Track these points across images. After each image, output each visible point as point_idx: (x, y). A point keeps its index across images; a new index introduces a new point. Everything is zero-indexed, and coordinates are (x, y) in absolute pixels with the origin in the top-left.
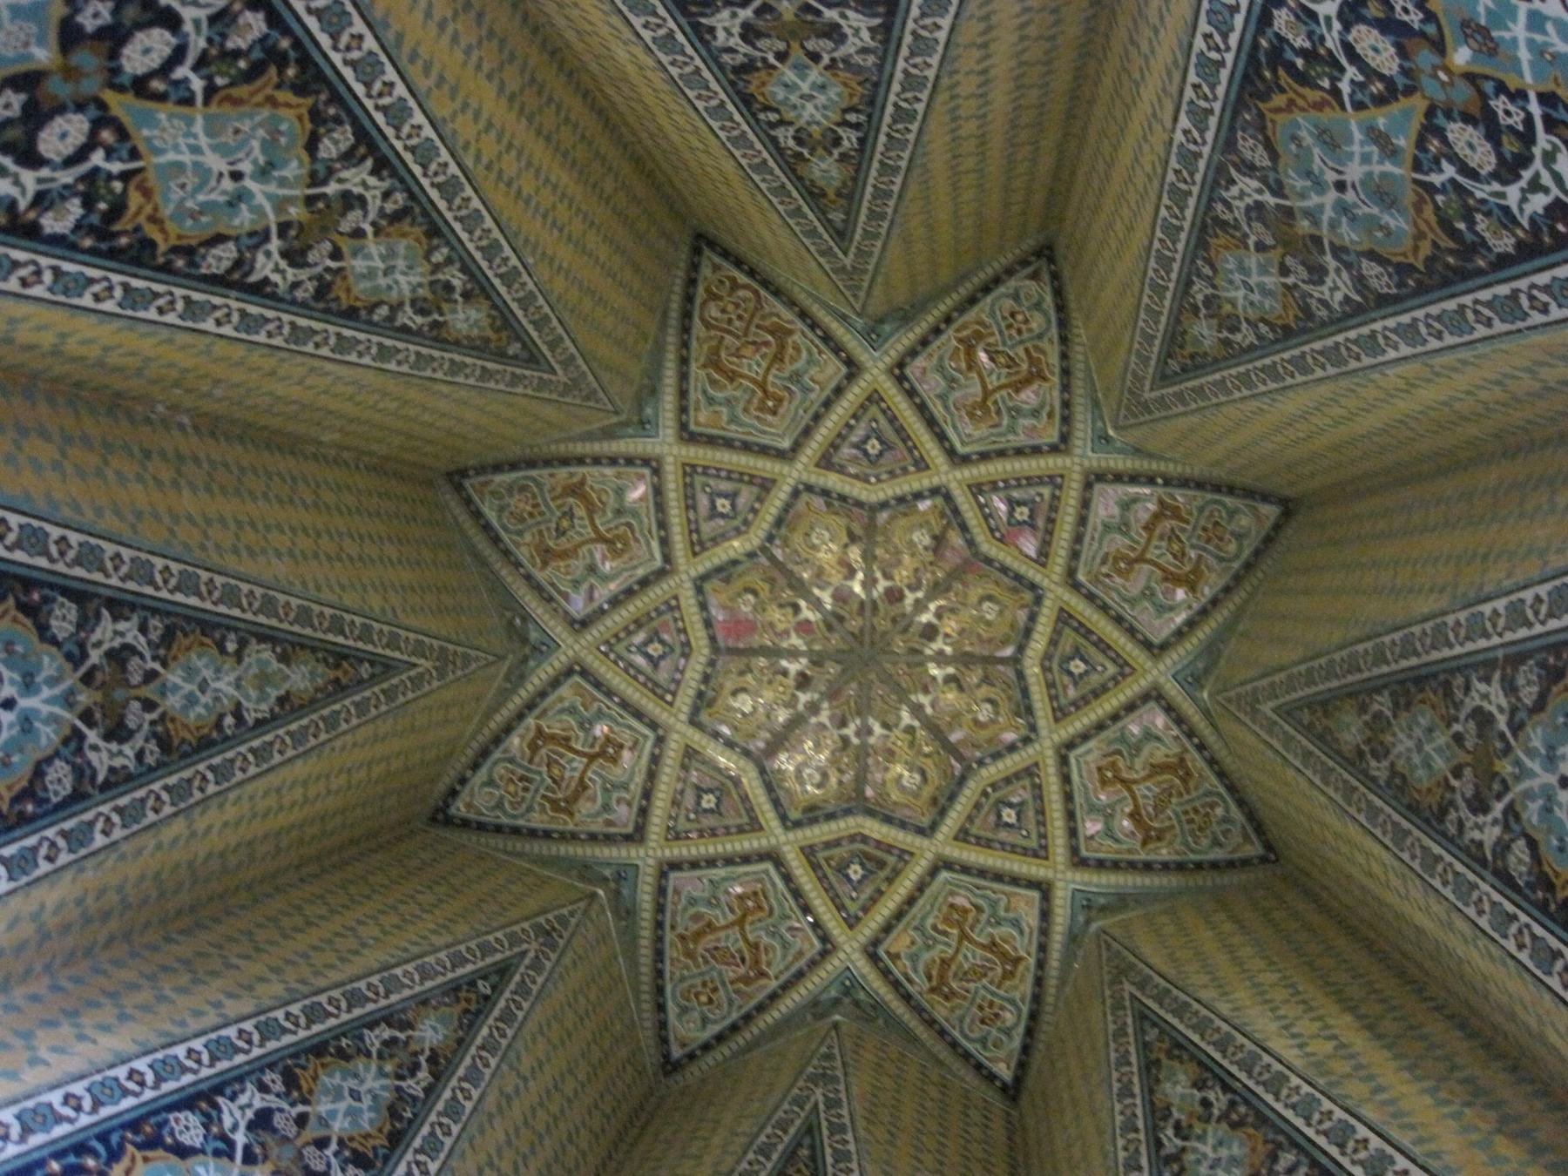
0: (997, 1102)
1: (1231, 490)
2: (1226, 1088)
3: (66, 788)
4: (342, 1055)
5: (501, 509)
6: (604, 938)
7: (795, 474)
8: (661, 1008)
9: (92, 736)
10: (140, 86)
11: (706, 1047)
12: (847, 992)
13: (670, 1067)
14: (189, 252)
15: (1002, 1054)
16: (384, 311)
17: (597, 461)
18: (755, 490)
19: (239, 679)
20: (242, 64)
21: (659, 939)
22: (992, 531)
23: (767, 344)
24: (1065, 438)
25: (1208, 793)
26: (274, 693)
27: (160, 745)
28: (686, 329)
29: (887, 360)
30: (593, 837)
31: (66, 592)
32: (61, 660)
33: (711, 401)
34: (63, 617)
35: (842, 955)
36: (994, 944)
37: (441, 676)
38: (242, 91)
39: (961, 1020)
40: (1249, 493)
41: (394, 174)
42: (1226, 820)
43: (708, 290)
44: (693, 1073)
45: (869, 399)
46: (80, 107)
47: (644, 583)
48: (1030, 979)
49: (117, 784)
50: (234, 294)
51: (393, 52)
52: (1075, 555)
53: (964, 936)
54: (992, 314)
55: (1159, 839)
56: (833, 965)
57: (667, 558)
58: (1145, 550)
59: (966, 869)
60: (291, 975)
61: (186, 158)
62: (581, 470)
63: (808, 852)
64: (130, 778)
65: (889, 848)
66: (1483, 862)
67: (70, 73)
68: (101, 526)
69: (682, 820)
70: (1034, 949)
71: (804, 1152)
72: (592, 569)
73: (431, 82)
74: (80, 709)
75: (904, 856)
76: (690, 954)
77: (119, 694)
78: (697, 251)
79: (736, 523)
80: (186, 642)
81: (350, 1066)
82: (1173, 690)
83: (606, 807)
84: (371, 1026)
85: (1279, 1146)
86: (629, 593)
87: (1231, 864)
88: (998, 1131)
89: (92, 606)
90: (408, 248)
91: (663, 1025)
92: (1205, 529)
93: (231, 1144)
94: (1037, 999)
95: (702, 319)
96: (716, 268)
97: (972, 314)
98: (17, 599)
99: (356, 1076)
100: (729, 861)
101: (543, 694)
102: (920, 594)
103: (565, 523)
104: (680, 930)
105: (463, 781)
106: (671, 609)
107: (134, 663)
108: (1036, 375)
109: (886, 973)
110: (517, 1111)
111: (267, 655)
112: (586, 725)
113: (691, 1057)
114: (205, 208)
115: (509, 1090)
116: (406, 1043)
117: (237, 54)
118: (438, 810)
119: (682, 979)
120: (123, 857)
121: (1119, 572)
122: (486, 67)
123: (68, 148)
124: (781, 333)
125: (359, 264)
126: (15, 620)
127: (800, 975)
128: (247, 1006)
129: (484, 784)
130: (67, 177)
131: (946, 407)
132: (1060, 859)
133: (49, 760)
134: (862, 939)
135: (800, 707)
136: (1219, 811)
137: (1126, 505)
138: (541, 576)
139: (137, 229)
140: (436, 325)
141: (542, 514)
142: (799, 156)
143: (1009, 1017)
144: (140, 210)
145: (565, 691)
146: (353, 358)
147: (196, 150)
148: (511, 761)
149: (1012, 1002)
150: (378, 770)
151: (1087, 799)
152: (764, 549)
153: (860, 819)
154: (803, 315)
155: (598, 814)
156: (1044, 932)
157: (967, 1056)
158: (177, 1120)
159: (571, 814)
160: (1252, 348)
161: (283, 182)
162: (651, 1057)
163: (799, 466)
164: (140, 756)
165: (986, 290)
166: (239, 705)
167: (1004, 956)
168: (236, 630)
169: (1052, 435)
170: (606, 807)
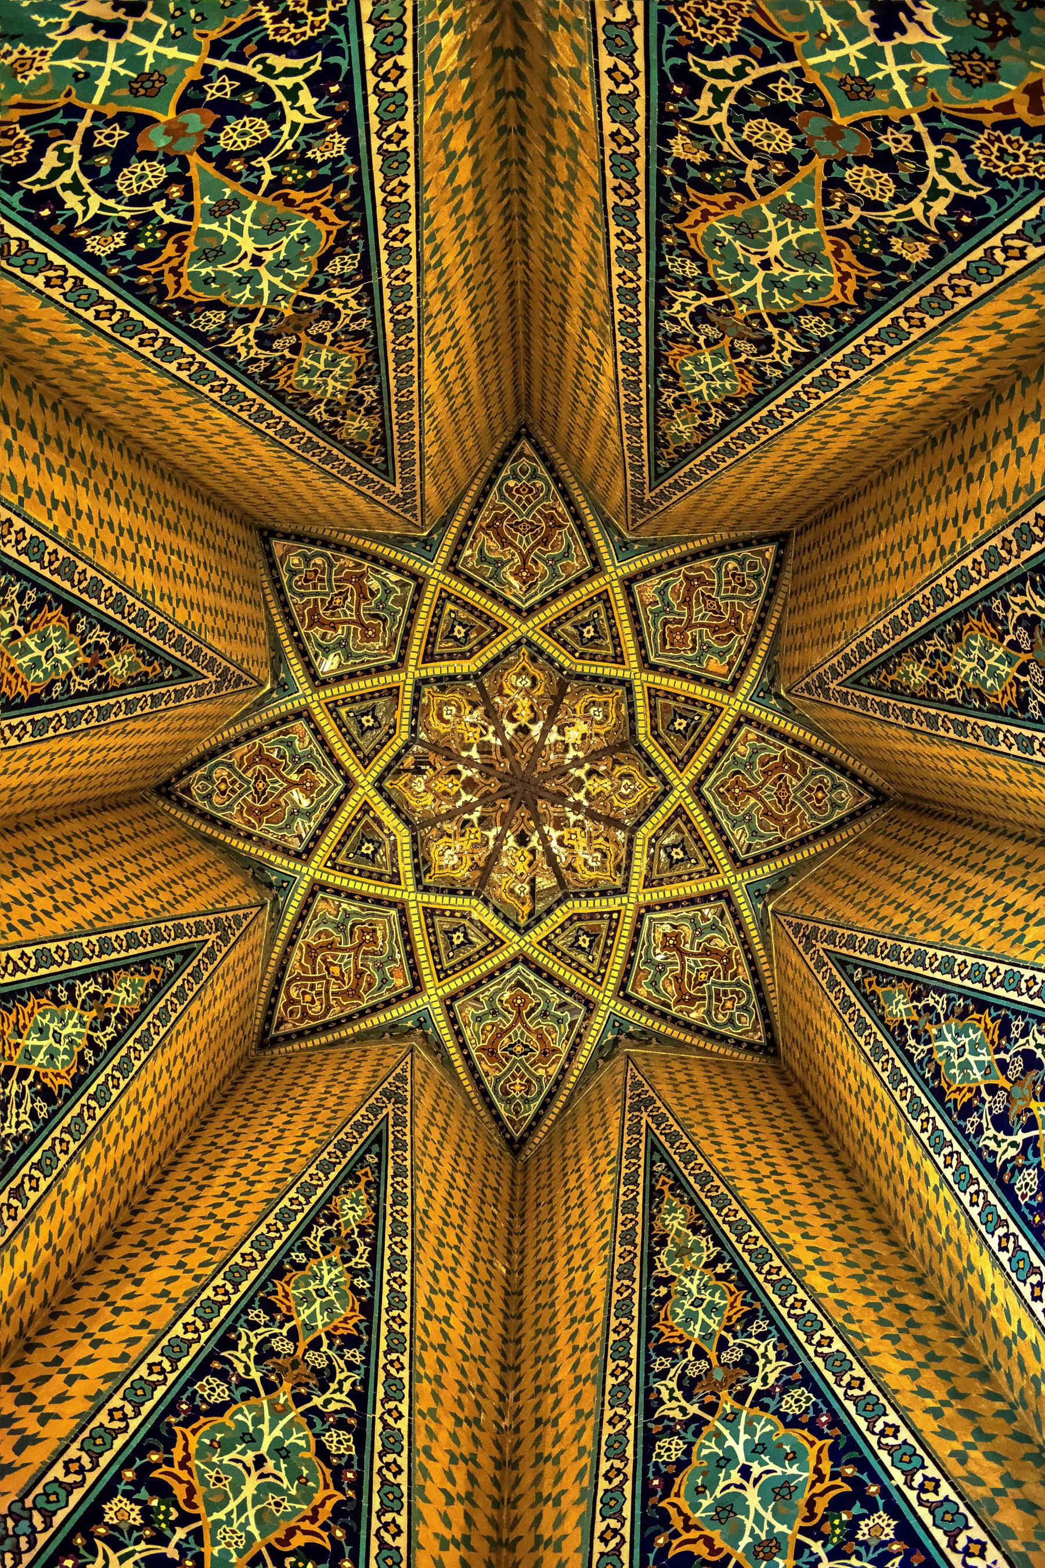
0: (793, 547)
1: (277, 581)
2: (659, 395)
4: (937, 1075)
5: (527, 1101)
6: (798, 891)
7: (413, 896)
8: (841, 823)
11: (854, 777)
12: (768, 692)
13: (880, 798)
14: (337, 1473)
15: (759, 560)
16: (359, 1282)
17: (463, 1046)
18: (437, 919)
19: (687, 1274)
20: (155, 1503)
21: (793, 847)
22: (391, 736)
23: (324, 960)
24: (298, 715)
25: (502, 497)
26: (692, 1238)
27: (750, 1323)
28: (338, 1023)
29: (298, 867)
30: (740, 928)
32: (701, 1440)
33: (384, 981)
35: (744, 707)
36: (684, 602)
37: (652, 1101)
38: (180, 1492)
39: (748, 600)
40: (272, 566)
41: (232, 1329)
42: (515, 477)
43: (301, 1020)
44: (876, 779)
45: (333, 868)
47: (538, 971)
48: (696, 564)
49: (790, 1348)
50: (369, 1416)
51: (121, 1377)
52: (380, 670)
53: (690, 626)
54: (230, 807)
55: (552, 517)
56: (752, 710)
57: (514, 962)
58: (353, 622)
59: (642, 645)
60: (899, 1136)
61: (251, 1512)
62: (474, 1053)
63: (681, 764)
64: (782, 1339)
65: (653, 708)
66: (368, 289)
69: (699, 868)
70: (675, 571)
71: (872, 680)
72: (545, 1014)
73: (143, 1333)
74: (737, 1406)
75: (653, 694)
76: (793, 820)
77: (718, 1375)
78: (275, 1042)
79: (466, 923)
80: (667, 1332)
81: (942, 1063)
82: (443, 556)
83: (714, 927)
84: (910, 1056)
85: (665, 336)
86: (551, 979)
87: (545, 458)
88: (810, 537)
89: (656, 1428)
90: (296, 1288)
91: (852, 816)
92: (315, 586)
93: (1026, 1141)
94: (708, 552)
95: (325, 1015)
96: (282, 1022)
97: (237, 822)
98: (661, 1499)
99: (948, 1056)
100: (714, 820)
101: (651, 1010)
102: (460, 767)
103: (519, 1049)
104: (779, 834)
105: (738, 1043)
106: (549, 942)
107: (693, 1372)
108: (260, 756)
109: (742, 669)
110: (935, 911)
111: (663, 1258)
112: (661, 969)
113: (865, 785)
114: (294, 1475)
115: (921, 925)
116: (914, 1023)
117: (147, 1512)
118: (767, 1053)
119: (813, 816)
121: (376, 634)
122: (130, 1288)
124: (312, 952)
125: (320, 1321)
126: (677, 1495)
127: (772, 732)
128: (928, 1166)
129: (735, 1027)
131: (315, 809)
132: (602, 581)
133: (782, 1416)
134: (726, 698)
135: (581, 817)
136: (511, 483)
137: (327, 651)
138: (564, 1049)
139: (325, 1527)
140: (362, 1234)
141: (518, 1070)
142: (120, 1019)
143: (732, 565)
144: (306, 1532)
145: (643, 993)
146: (406, 1289)
147: (242, 1508)
148: (708, 1012)
149: (719, 571)
150: (739, 1120)
151: (550, 582)
152: (478, 895)
153: (641, 738)
154: (291, 942)
155: (721, 931)
156: (658, 569)
157: (773, 584)
158: (1024, 1196)
159: (730, 951)
160: (105, 627)
161: (258, 1420)
162: (878, 816)
163: (405, 896)
165: (213, 820)
166: (706, 1266)
167: (689, 590)
168: (649, 1291)
169: (300, 725)
170: (714, 927)
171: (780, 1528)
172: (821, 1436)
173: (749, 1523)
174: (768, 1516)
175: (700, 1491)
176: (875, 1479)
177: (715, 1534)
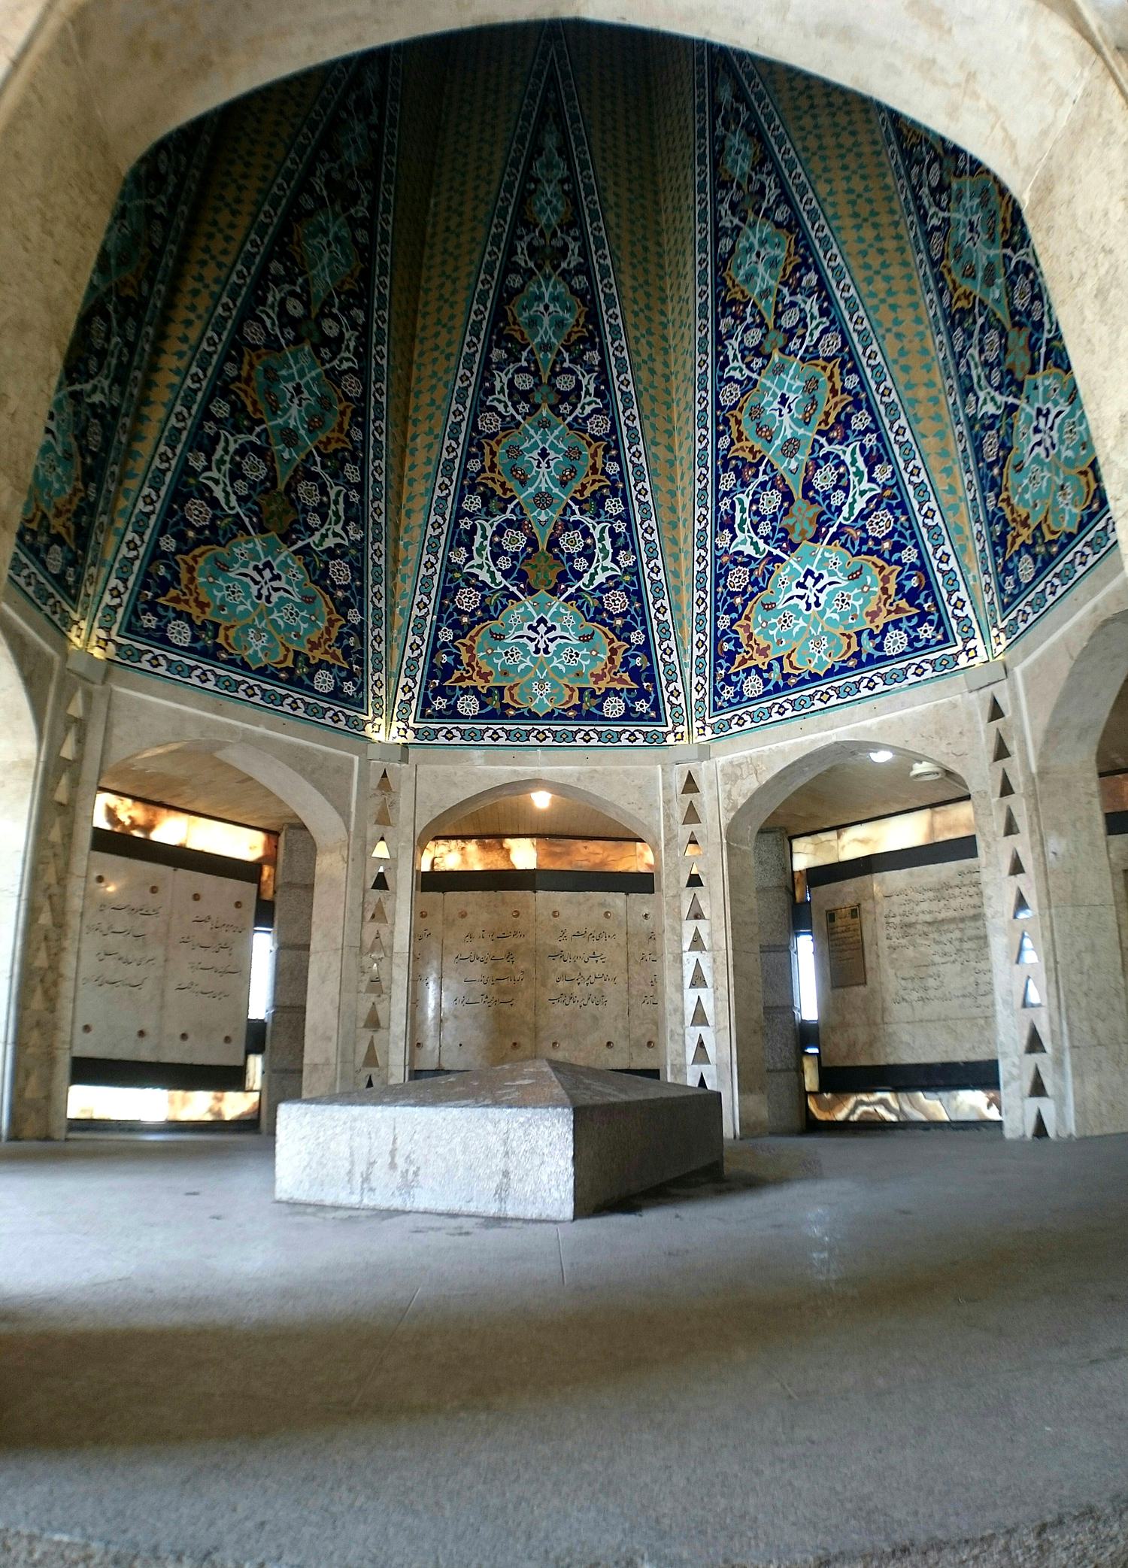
3: (583, 278)
9: (564, 265)
10: (307, 305)
31: (503, 281)
34: (515, 280)
46: (319, 326)
67: (310, 334)
68: (477, 262)
77: (548, 251)
81: (727, 148)
107: (535, 243)
114: (344, 253)
120: (618, 247)
123: (334, 324)
125: (354, 160)
130: (344, 320)
133: (571, 287)
147: (323, 269)
164: (575, 239)
171: (553, 340)
172: (585, 305)
173: (541, 332)
174: (550, 333)
175: (524, 309)
176: (600, 337)
177: (526, 332)
